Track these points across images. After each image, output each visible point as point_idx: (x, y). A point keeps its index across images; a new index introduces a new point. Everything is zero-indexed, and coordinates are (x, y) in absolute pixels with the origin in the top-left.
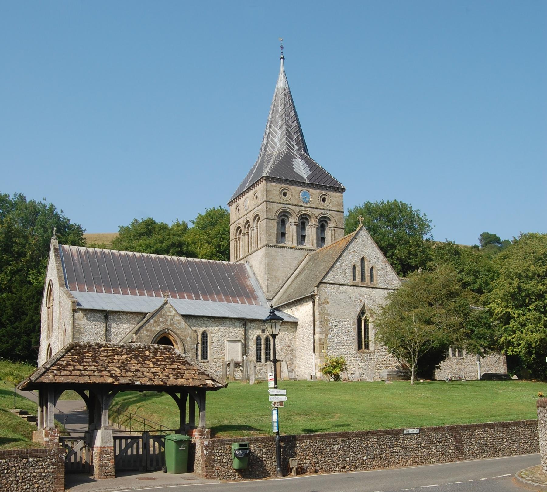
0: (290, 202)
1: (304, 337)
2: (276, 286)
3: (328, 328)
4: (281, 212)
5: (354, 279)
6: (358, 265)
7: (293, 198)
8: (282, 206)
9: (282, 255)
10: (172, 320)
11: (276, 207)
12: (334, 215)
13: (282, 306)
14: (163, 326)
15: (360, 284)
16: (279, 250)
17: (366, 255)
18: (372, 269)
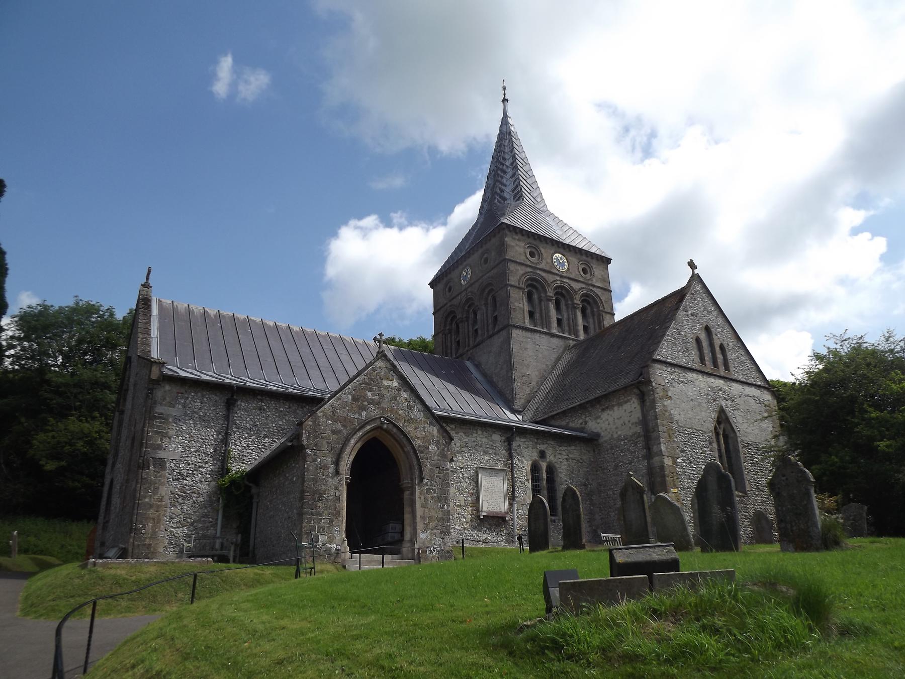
0: (540, 267)
1: (617, 467)
2: (528, 390)
3: (675, 445)
4: (527, 280)
5: (702, 360)
6: (703, 336)
7: (544, 262)
8: (529, 270)
9: (535, 343)
10: (395, 397)
11: (521, 270)
12: (599, 294)
13: (553, 417)
14: (374, 412)
15: (709, 370)
16: (529, 334)
17: (711, 324)
18: (722, 347)
